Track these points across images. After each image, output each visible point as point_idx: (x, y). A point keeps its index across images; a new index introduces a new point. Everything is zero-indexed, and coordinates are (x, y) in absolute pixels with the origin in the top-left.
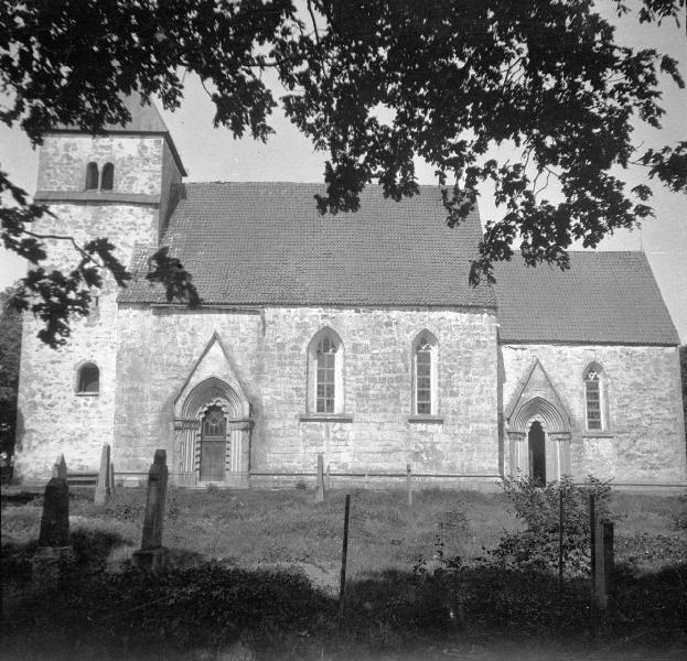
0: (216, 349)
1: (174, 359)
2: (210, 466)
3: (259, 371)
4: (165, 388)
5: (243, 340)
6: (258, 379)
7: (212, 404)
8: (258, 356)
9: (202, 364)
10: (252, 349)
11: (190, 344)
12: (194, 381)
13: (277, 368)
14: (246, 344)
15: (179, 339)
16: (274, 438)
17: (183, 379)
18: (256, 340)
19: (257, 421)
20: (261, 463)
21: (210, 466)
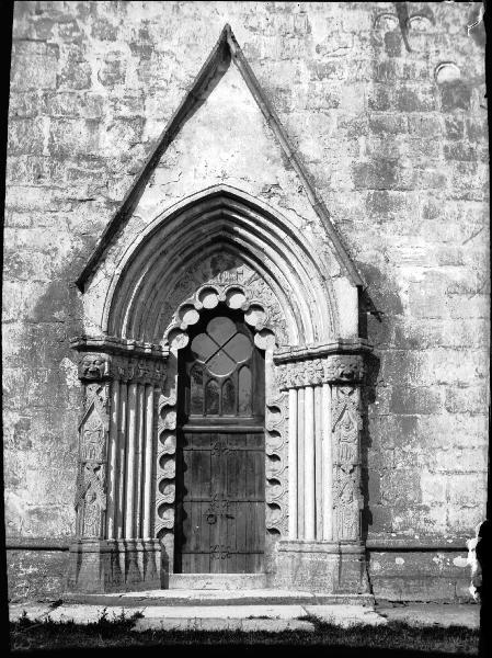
0: (230, 93)
1: (78, 133)
2: (211, 518)
3: (381, 176)
4: (43, 239)
5: (322, 73)
6: (381, 207)
7: (211, 302)
8: (378, 127)
9: (180, 143)
10: (355, 98)
11: (132, 81)
12: (154, 206)
13: (447, 170)
14: (331, 85)
15: (95, 65)
16: (443, 418)
17: (110, 203)
18: (366, 71)
19: (387, 353)
20: (402, 509)
21: (211, 518)
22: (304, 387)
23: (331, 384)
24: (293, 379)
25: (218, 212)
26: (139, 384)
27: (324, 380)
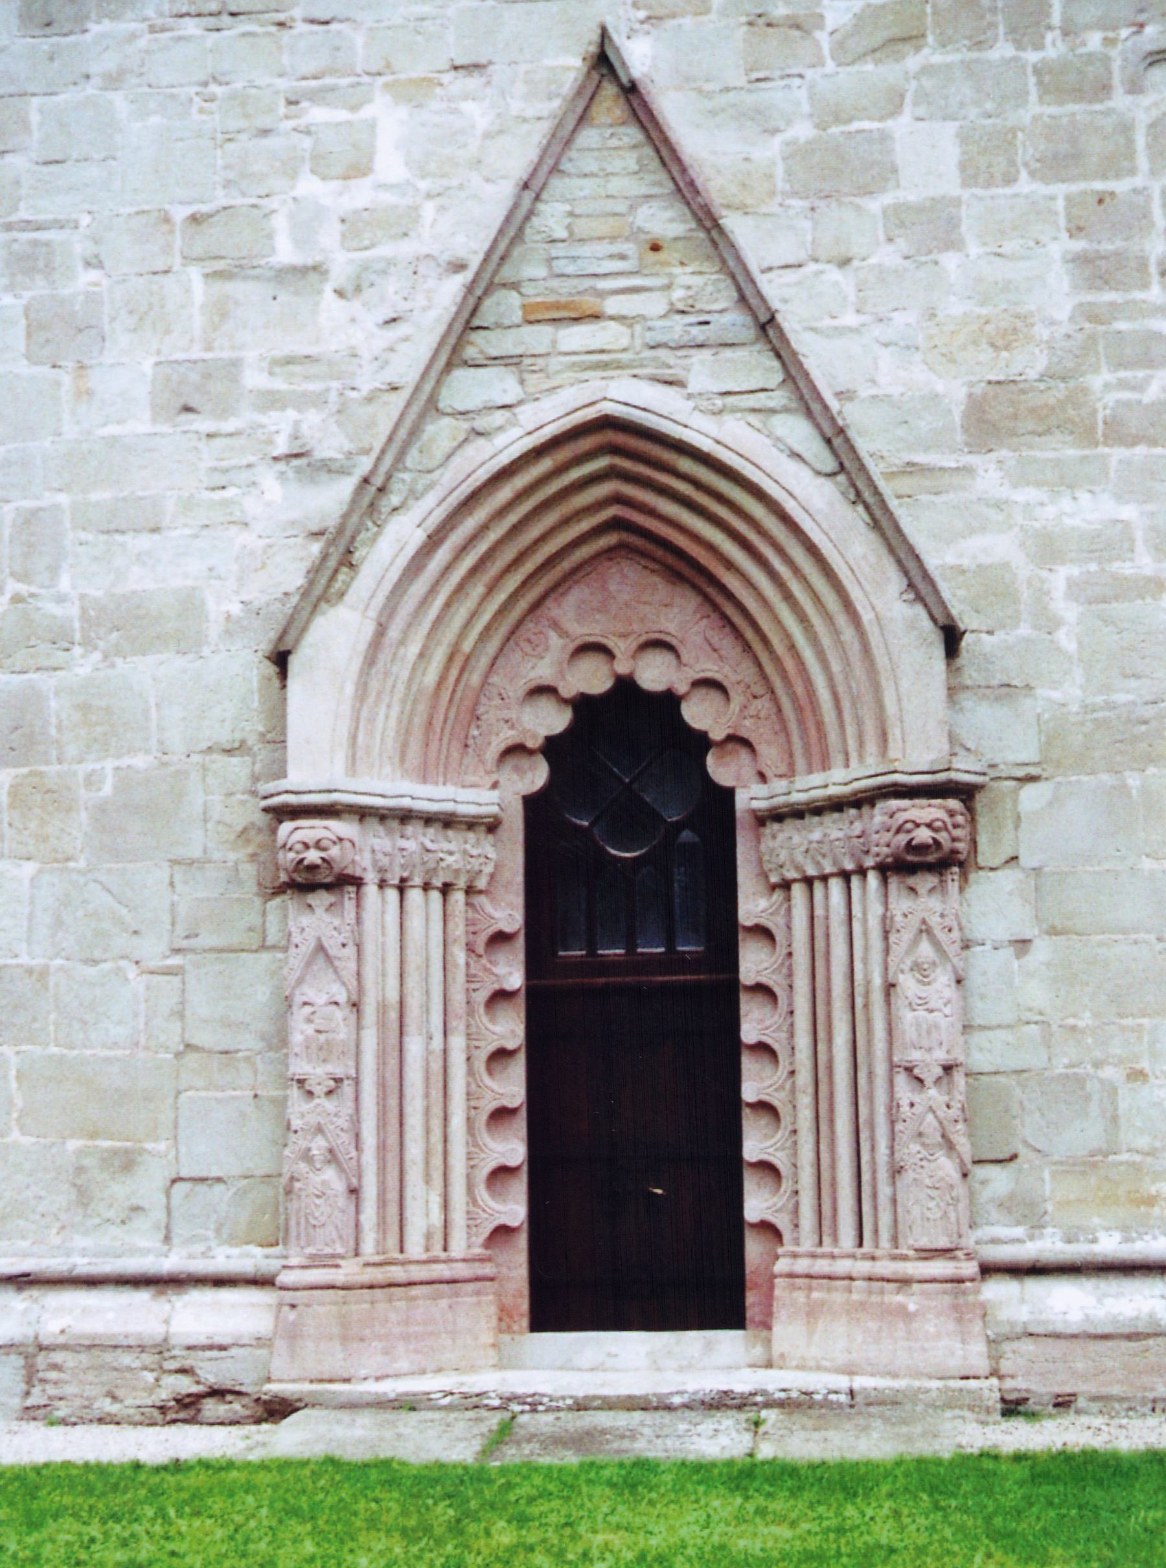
22: (824, 878)
23: (884, 869)
24: (800, 858)
25: (600, 463)
26: (426, 887)
27: (869, 862)
